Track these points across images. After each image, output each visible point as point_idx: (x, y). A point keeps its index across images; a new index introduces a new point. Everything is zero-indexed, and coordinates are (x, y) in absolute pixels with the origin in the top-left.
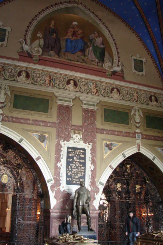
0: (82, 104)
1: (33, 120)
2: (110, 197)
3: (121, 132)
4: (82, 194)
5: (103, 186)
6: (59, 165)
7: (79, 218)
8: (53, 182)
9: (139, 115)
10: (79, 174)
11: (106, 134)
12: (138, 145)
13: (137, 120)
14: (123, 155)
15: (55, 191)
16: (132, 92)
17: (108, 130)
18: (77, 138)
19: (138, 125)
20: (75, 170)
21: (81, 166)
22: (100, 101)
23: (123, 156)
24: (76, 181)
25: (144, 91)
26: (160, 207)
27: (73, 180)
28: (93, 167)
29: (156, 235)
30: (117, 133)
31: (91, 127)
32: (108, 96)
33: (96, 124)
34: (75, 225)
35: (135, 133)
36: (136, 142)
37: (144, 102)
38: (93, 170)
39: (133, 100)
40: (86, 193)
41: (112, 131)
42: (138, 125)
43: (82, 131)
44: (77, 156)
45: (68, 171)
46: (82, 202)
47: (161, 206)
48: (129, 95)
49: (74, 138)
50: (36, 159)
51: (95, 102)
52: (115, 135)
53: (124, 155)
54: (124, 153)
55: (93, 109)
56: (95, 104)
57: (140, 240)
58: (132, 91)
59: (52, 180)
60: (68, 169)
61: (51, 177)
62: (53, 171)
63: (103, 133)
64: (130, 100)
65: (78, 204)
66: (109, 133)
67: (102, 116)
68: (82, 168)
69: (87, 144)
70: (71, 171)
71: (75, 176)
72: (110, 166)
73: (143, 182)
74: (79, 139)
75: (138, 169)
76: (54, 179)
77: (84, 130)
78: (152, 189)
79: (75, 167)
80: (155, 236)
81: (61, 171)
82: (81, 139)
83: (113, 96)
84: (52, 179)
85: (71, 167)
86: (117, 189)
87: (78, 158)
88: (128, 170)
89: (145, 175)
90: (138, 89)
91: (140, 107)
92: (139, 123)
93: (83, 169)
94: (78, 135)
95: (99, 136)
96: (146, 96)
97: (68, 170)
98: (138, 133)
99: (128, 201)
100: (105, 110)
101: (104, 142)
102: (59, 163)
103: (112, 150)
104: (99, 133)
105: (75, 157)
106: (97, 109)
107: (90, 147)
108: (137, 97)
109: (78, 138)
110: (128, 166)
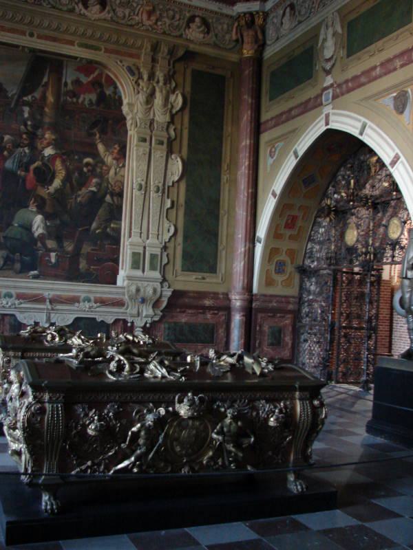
1: (382, 64)
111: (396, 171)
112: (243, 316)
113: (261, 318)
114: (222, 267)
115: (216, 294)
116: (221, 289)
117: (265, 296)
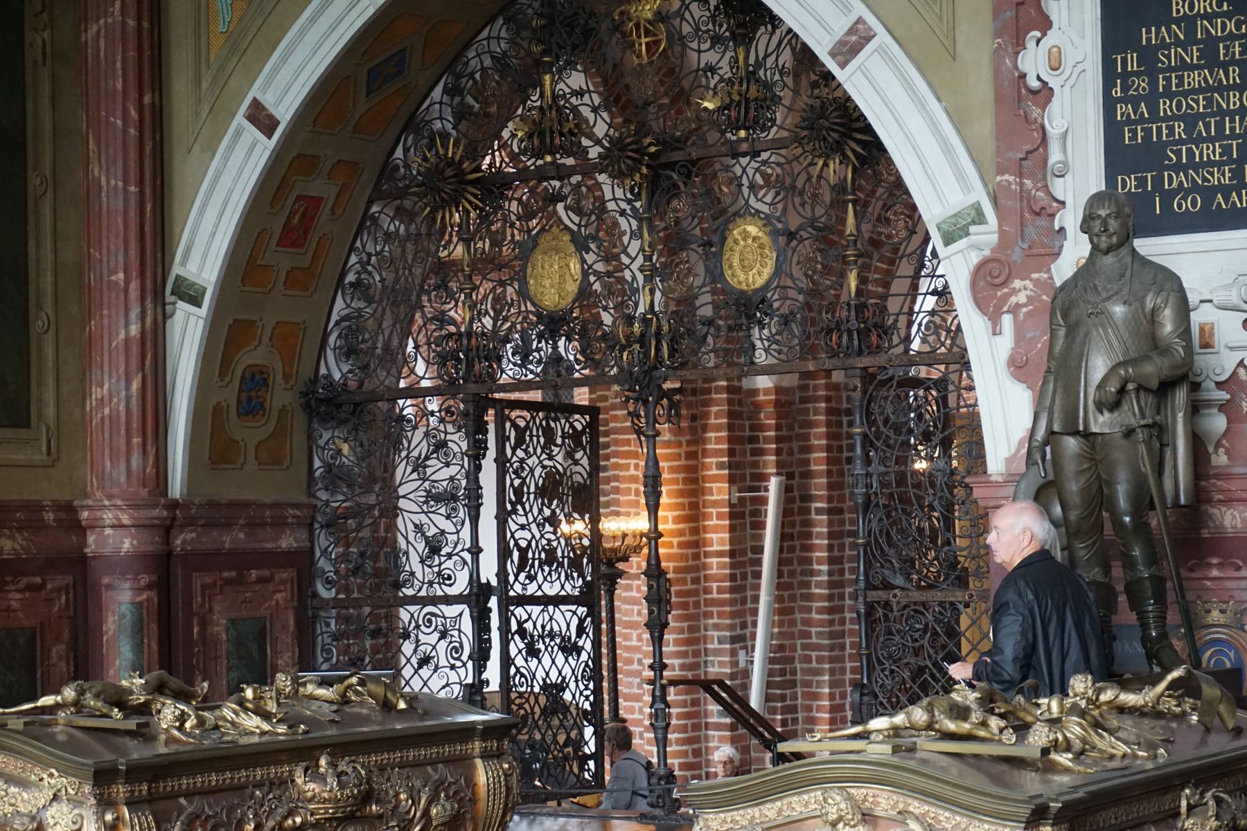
6: (1033, 62)
8: (987, 235)
10: (1232, 114)
15: (1014, 310)
20: (1193, 79)
24: (1209, 193)
27: (1171, 180)
34: (1215, 616)
45: (1125, 100)
50: (832, 54)
59: (980, 218)
60: (1125, 88)
61: (967, 188)
62: (985, 126)
70: (1152, 100)
71: (1199, 140)
76: (995, 201)
81: (1056, 119)
84: (978, 209)
85: (1148, 57)
97: (1117, 92)
102: (1031, 45)
111: (859, 79)
112: (150, 587)
113: (204, 587)
114: (46, 400)
115: (35, 508)
116: (47, 490)
117: (213, 505)
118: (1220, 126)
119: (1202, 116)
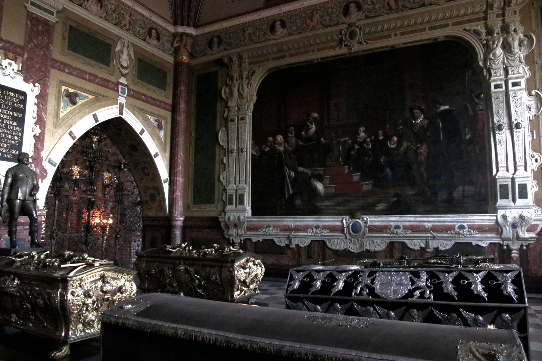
0: (28, 4)
2: (59, 188)
3: (96, 76)
4: (22, 179)
5: (55, 167)
7: (14, 222)
9: (129, 55)
10: (9, 139)
11: (68, 73)
12: (120, 105)
13: (125, 62)
14: (94, 117)
16: (122, 11)
17: (72, 67)
18: (10, 68)
19: (124, 71)
21: (15, 124)
22: (64, 9)
23: (95, 119)
25: (141, 15)
26: (137, 210)
28: (38, 131)
29: (174, 251)
30: (88, 77)
31: (42, 53)
32: (79, 3)
33: (51, 51)
35: (119, 83)
36: (118, 100)
37: (139, 34)
38: (37, 135)
39: (122, 25)
40: (30, 177)
41: (79, 69)
42: (124, 71)
43: (23, 56)
44: (8, 103)
46: (22, 193)
47: (139, 209)
48: (116, 14)
49: (4, 67)
51: (54, 8)
52: (85, 79)
53: (95, 118)
54: (95, 114)
55: (49, 19)
56: (55, 11)
57: (145, 259)
58: (122, 9)
63: (64, 71)
64: (117, 24)
65: (12, 197)
66: (75, 73)
67: (64, 38)
68: (17, 129)
69: (31, 84)
72: (71, 134)
73: (117, 168)
74: (16, 71)
75: (110, 146)
77: (25, 56)
78: (127, 181)
79: (3, 126)
80: (172, 252)
82: (18, 72)
83: (90, 6)
86: (73, 175)
87: (9, 108)
88: (94, 146)
89: (121, 157)
90: (132, 9)
91: (133, 42)
92: (126, 68)
93: (19, 132)
94: (13, 62)
95: (55, 74)
96: (143, 25)
98: (122, 84)
99: (90, 197)
100: (71, 28)
101: (64, 88)
103: (76, 106)
104: (54, 68)
105: (4, 104)
106: (57, 22)
107: (37, 90)
108: (130, 22)
109: (13, 70)
110: (95, 139)
118: (7, 141)
119: (3, 138)
